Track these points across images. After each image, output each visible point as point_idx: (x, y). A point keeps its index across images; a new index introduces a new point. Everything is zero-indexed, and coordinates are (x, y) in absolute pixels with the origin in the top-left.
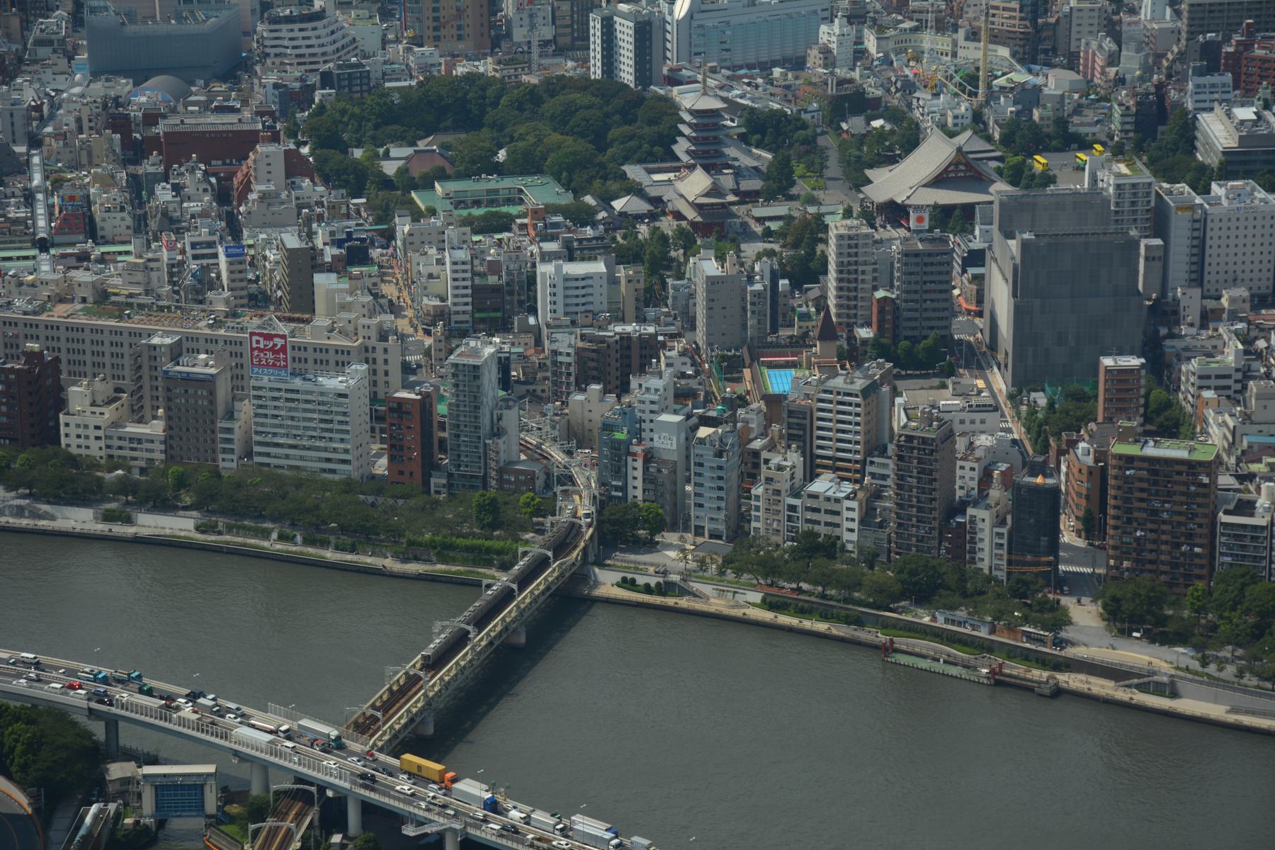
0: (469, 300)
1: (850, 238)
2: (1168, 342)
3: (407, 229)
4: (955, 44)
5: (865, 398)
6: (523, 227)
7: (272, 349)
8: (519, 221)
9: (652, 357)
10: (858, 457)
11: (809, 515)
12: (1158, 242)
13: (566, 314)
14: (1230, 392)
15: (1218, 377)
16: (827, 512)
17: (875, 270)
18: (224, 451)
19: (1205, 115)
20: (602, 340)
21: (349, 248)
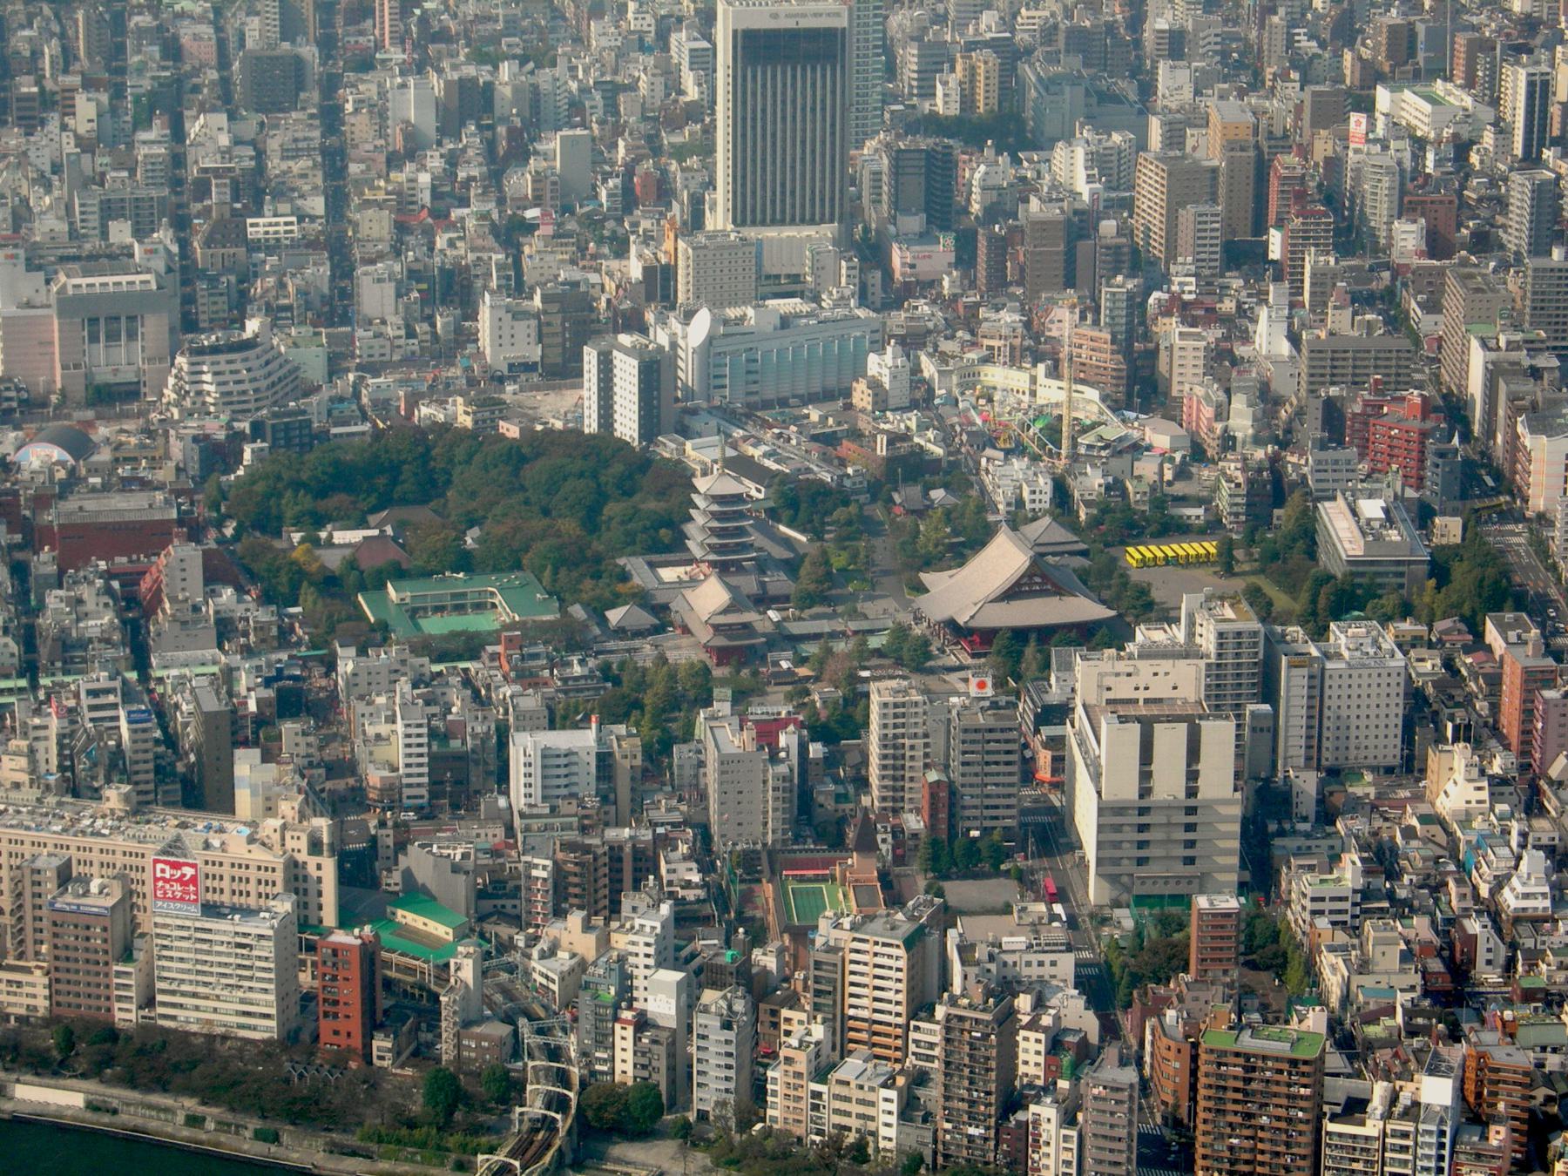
0: (425, 770)
1: (896, 705)
2: (1278, 842)
3: (350, 667)
4: (1034, 380)
5: (908, 949)
6: (494, 657)
7: (180, 880)
8: (490, 649)
9: (648, 871)
10: (900, 1020)
11: (838, 1105)
12: (1267, 707)
13: (545, 798)
14: (1347, 918)
15: (1332, 899)
16: (861, 1102)
17: (926, 745)
18: (120, 999)
19: (1327, 504)
20: (587, 849)
21: (279, 690)
